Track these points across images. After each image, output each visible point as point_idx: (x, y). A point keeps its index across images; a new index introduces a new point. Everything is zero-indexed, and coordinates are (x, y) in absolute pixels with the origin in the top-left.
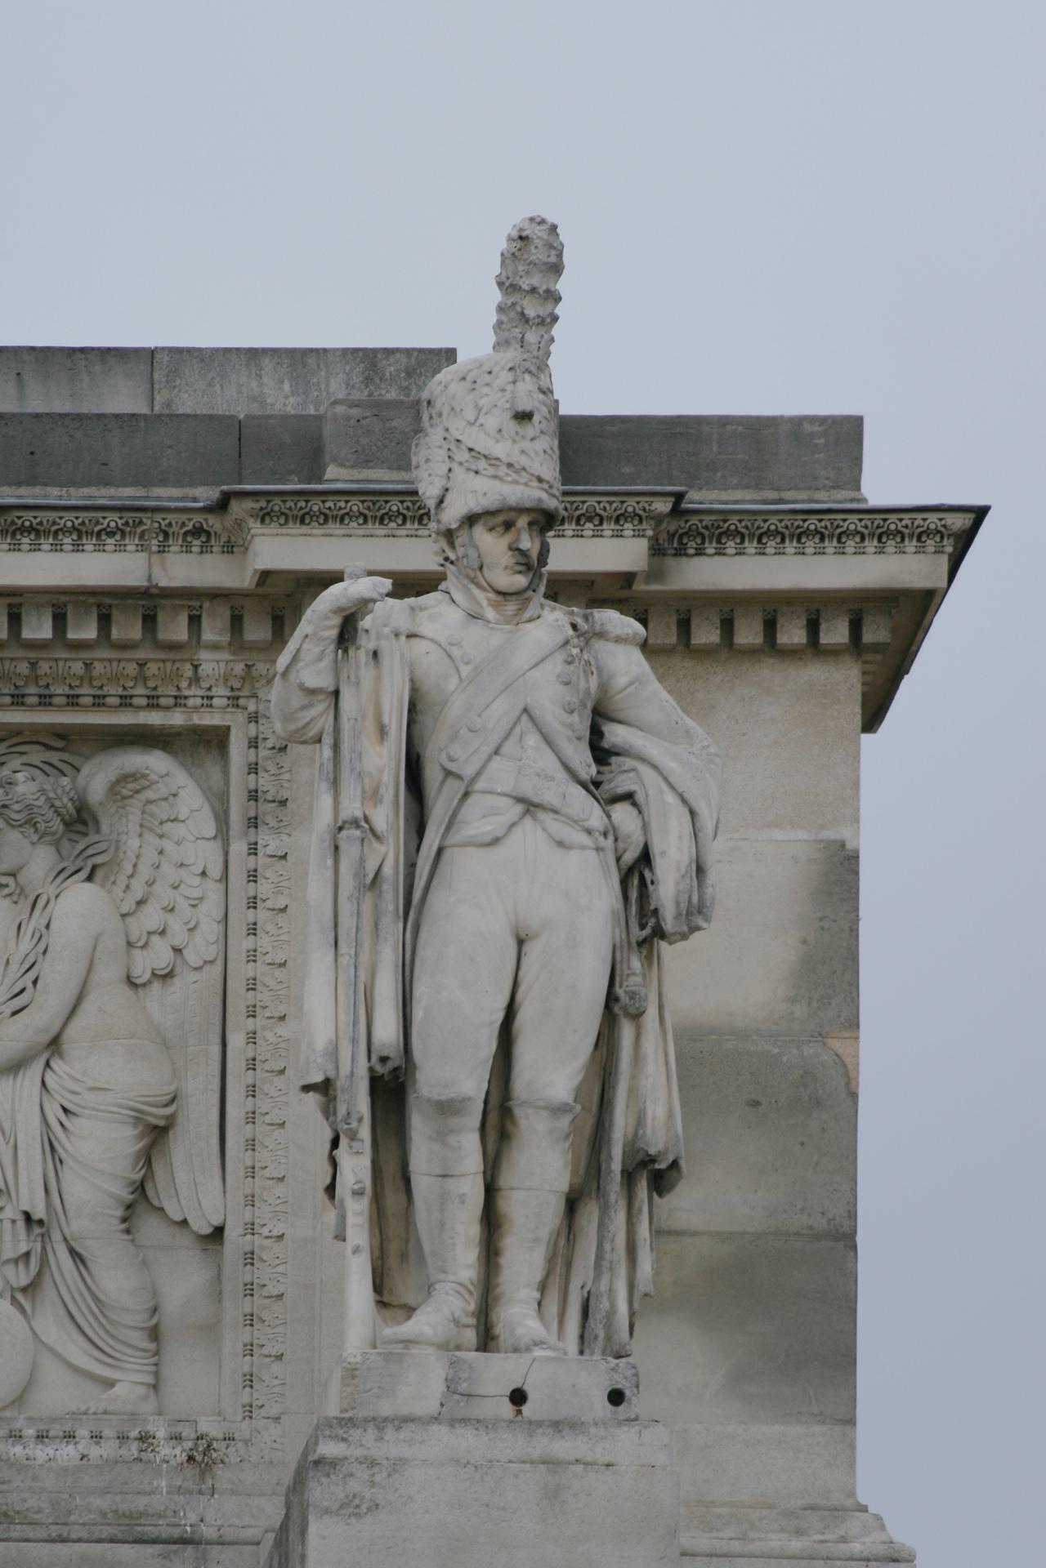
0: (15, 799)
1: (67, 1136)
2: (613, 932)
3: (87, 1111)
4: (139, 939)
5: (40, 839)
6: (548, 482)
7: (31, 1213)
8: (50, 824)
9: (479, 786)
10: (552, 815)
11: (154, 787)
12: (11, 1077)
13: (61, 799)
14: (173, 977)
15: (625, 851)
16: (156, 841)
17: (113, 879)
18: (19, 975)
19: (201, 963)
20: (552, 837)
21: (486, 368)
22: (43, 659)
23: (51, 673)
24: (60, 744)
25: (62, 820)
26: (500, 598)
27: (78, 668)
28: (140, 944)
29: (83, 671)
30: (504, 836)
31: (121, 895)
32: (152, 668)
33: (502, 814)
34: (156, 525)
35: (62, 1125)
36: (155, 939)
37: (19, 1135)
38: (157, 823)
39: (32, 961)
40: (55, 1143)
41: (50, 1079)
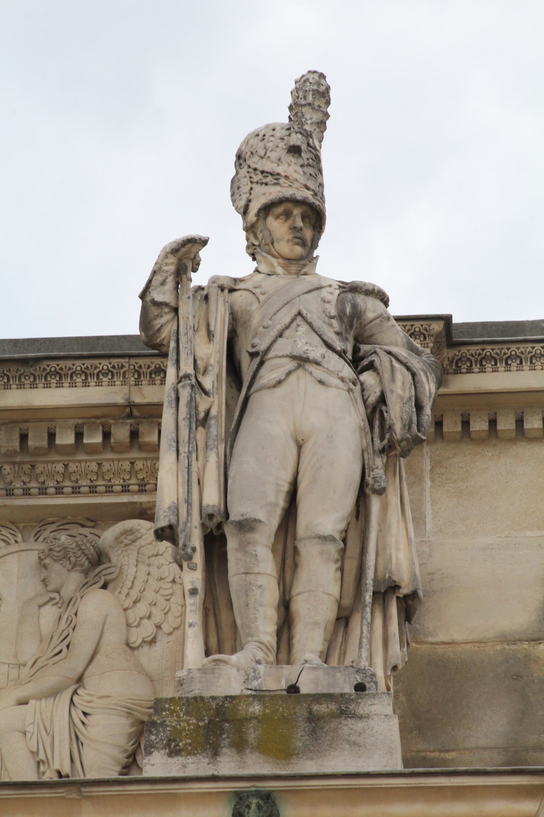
0: (57, 545)
1: (85, 728)
2: (362, 441)
3: (96, 710)
4: (135, 621)
5: (73, 568)
6: (313, 190)
7: (61, 771)
8: (79, 559)
9: (271, 354)
10: (315, 366)
11: (144, 537)
12: (52, 699)
13: (85, 545)
14: (155, 642)
15: (369, 397)
16: (146, 569)
17: (119, 590)
18: (58, 642)
19: (171, 630)
20: (316, 379)
21: (271, 127)
22: (72, 461)
23: (77, 471)
24: (92, 524)
25: (88, 558)
26: (286, 262)
27: (93, 466)
28: (135, 624)
29: (97, 468)
30: (284, 380)
31: (124, 598)
32: (139, 465)
33: (283, 367)
34: (132, 367)
35: (83, 723)
36: (145, 621)
37: (55, 729)
38: (146, 558)
39: (67, 634)
40: (79, 734)
41: (76, 699)
